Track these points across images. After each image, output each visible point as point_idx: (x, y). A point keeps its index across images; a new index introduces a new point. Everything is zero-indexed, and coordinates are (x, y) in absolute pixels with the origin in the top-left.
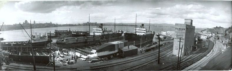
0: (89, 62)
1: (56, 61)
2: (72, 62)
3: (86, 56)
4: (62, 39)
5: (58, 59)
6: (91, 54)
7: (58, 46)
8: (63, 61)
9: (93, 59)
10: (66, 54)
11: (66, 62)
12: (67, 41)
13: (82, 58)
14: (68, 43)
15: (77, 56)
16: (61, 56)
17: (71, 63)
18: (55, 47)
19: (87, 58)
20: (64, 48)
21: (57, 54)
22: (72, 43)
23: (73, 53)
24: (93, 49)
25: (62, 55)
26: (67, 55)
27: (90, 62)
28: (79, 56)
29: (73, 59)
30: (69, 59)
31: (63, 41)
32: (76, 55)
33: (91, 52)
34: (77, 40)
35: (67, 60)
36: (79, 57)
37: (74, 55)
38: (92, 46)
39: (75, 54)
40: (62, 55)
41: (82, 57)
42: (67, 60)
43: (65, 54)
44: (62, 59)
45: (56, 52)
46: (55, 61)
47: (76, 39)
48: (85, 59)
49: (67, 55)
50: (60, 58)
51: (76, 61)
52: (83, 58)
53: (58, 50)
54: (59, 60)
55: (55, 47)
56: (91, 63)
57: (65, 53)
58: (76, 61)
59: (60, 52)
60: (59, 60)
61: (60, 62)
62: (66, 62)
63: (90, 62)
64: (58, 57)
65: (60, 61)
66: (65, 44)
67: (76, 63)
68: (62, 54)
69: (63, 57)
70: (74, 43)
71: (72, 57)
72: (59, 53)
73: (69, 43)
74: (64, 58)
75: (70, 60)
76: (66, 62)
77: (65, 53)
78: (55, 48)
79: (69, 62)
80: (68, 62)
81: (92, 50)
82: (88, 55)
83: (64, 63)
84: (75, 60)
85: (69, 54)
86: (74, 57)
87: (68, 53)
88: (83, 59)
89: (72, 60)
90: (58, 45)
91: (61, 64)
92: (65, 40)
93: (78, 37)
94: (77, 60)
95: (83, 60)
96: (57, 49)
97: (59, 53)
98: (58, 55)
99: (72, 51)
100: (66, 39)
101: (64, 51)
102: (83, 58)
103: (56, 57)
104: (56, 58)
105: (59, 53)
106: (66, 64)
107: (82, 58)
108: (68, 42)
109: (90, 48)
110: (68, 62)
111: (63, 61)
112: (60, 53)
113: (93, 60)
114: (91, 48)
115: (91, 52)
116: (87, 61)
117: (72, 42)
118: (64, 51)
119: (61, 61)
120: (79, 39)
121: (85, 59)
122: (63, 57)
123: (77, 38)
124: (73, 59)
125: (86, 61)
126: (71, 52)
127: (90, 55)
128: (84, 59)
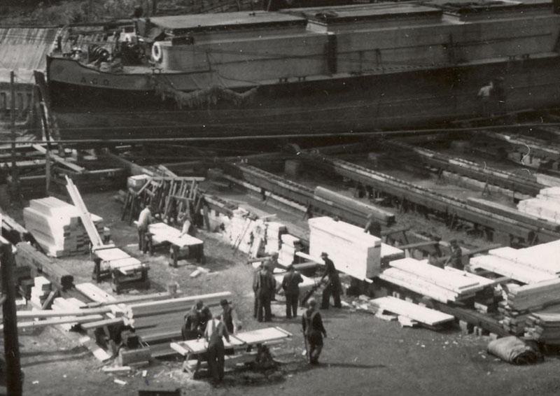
0: (492, 353)
1: (38, 331)
2: (262, 348)
3: (460, 263)
4: (126, 37)
5: (67, 307)
6: (518, 243)
7: (67, 135)
8: (134, 343)
9: (546, 307)
10: (182, 238)
11: (176, 347)
12: (188, 59)
13: (405, 293)
14: (204, 86)
15: (329, 268)
16: (102, 276)
17: (250, 366)
18: (24, 141)
19: (467, 300)
20: (150, 158)
21: (57, 245)
22: (263, 91)
23: (274, 227)
24: (546, 169)
25: (120, 260)
26: (195, 255)
27: (506, 346)
28: (361, 273)
29: (278, 309)
30: (217, 312)
31: (134, 54)
32: (315, 257)
33: (529, 207)
34: (330, 50)
35: (194, 327)
36: (358, 288)
37: (286, 259)
38: (537, 134)
39: (303, 246)
40: (120, 260)
41: (391, 289)
42: (194, 327)
43: (165, 247)
44: (122, 308)
45: (34, 208)
46: (27, 344)
47: (319, 30)
48: (434, 304)
49: (195, 255)
50: (100, 293)
51: (315, 333)
52: (416, 297)
53: (72, 189)
54: (78, 329)
55: (24, 141)
56: (523, 359)
57: (161, 232)
58: (315, 333)
59: (92, 209)
60: (78, 329)
61: (101, 354)
62: (176, 358)
63: (506, 346)
64: (67, 286)
65: (102, 344)
66: (171, 102)
67: (314, 362)
68: (120, 244)
69: (139, 281)
70: (284, 91)
71: (265, 289)
72: (75, 230)
73: (217, 92)
74: (149, 300)
75: (228, 329)
76: (176, 347)
77: (161, 232)
78: (27, 153)
79: (215, 353)
80: (199, 345)
81: (533, 191)
82: (478, 261)
83: (152, 363)
84: (297, 330)
85: (224, 236)
86: (292, 283)
87: (198, 223)
88: (409, 312)
89: (264, 316)
90: (68, 118)
91: (108, 382)
92: (160, 53)
93: (343, 12)
94: (333, 325)
95: (419, 326)
96: (58, 169)
97: (78, 222)
98: (64, 255)
99: (262, 202)
100: (183, 37)
101: (142, 200)
102: (416, 297)
103: (40, 281)
104: (37, 292)
105: (78, 222)
106: (182, 376)
107: (405, 293)
108: (199, 72)
109: (503, 156)
110: (199, 345)
111: (134, 343)
112: (90, 220)
113: (546, 326)
114: (528, 150)
115: (529, 207)
116: (463, 339)
117: (269, 76)
118: (142, 200)
119: (112, 335)
120: (364, 38)
121: (434, 304)
122: (139, 281)
123: (331, 21)
124: (278, 309)
125: (449, 341)
126: (242, 209)
127: (507, 251)
128: (434, 317)
